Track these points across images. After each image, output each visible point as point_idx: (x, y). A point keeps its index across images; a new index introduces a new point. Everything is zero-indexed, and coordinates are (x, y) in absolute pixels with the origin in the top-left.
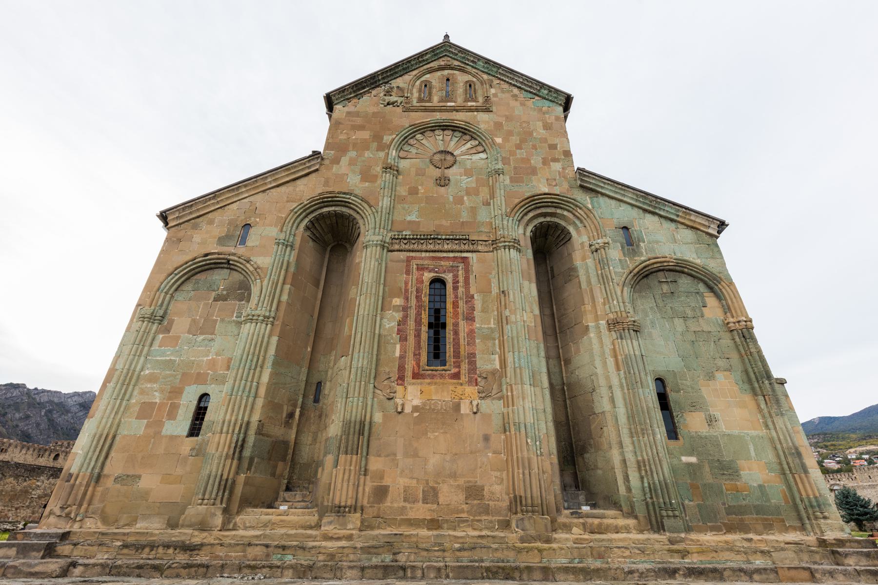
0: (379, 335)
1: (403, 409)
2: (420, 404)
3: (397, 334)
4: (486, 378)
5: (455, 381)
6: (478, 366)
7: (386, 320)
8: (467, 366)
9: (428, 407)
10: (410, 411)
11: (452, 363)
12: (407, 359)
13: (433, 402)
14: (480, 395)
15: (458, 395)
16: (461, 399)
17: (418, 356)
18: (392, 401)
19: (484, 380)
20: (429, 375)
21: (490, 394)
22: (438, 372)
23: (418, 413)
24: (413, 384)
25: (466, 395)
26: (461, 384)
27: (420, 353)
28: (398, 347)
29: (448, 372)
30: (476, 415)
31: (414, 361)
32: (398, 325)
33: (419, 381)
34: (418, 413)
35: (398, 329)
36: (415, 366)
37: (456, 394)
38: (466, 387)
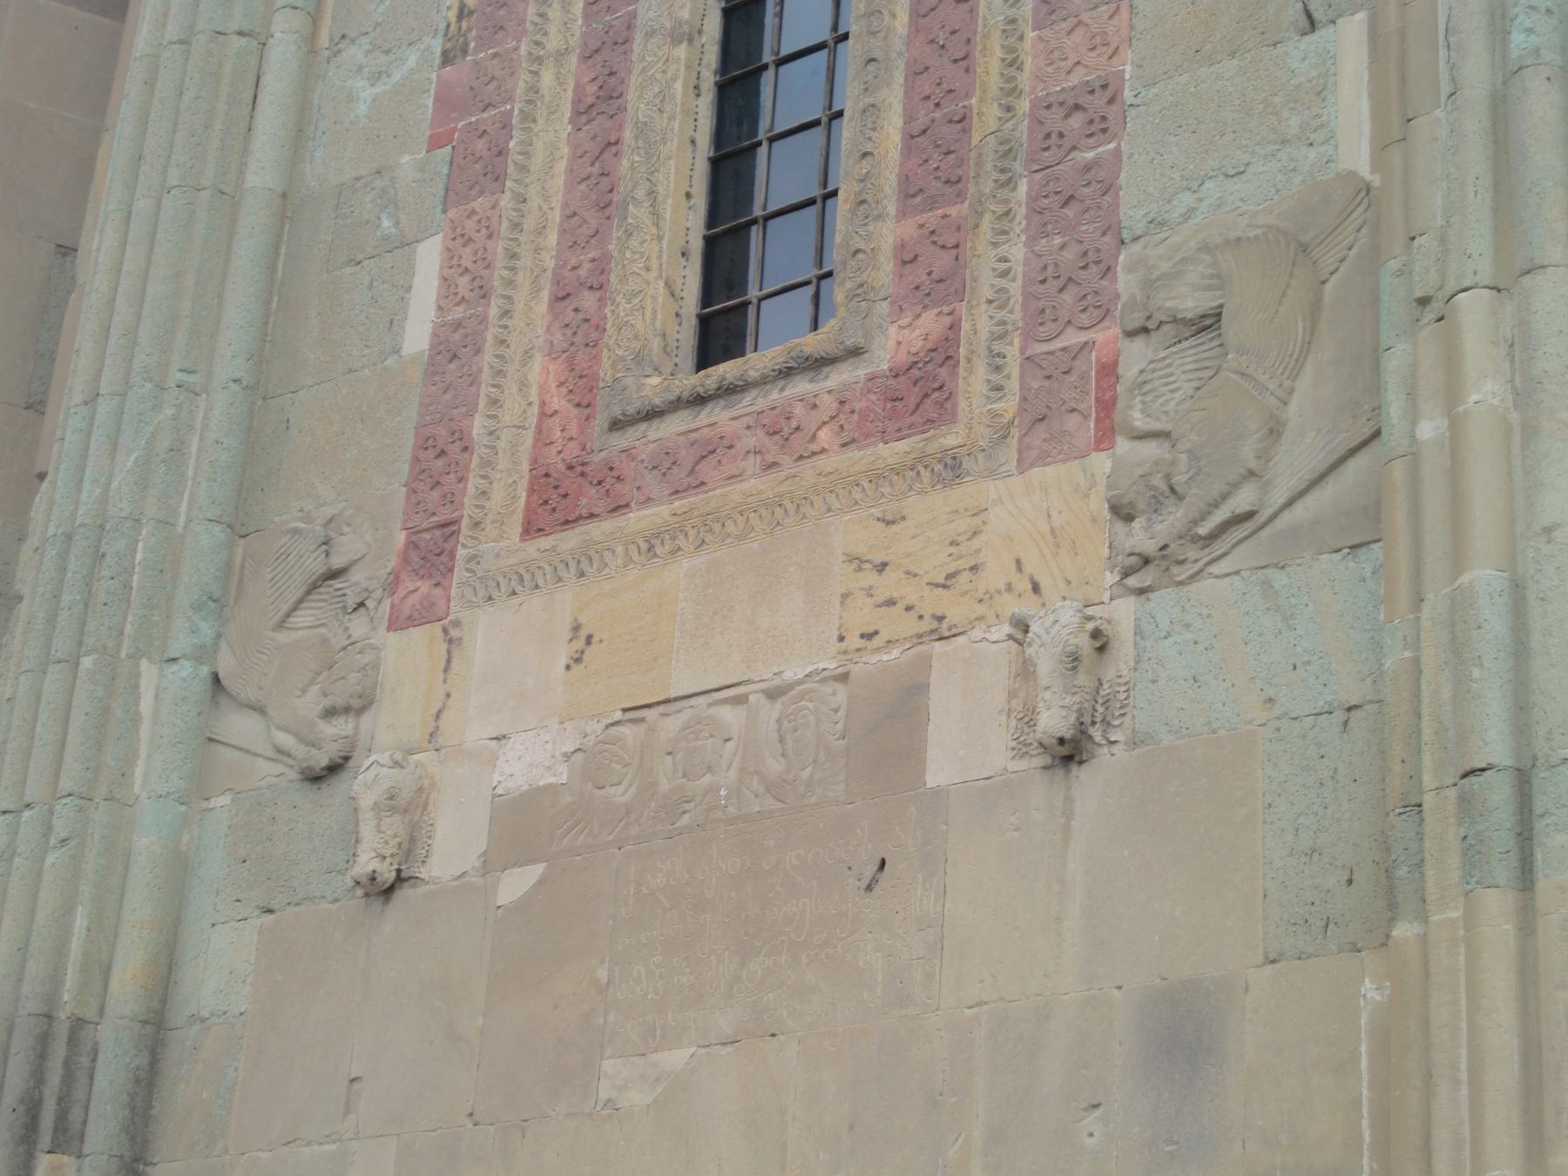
0: (287, 204)
1: (411, 847)
2: (562, 775)
3: (435, 143)
4: (1208, 323)
5: (893, 452)
6: (1132, 213)
7: (355, 53)
8: (1017, 252)
9: (620, 794)
10: (472, 861)
11: (884, 272)
12: (487, 358)
13: (670, 725)
14: (1140, 537)
15: (909, 593)
16: (941, 631)
17: (588, 300)
18: (340, 787)
19: (1189, 356)
20: (664, 462)
21: (1243, 500)
22: (750, 402)
23: (537, 870)
24: (523, 581)
25: (996, 573)
26: (952, 468)
27: (601, 266)
28: (429, 257)
29: (838, 377)
30: (1081, 773)
31: (551, 352)
32: (447, 59)
33: (569, 540)
34: (537, 870)
35: (446, 102)
36: (557, 402)
37: (887, 584)
38: (992, 489)
